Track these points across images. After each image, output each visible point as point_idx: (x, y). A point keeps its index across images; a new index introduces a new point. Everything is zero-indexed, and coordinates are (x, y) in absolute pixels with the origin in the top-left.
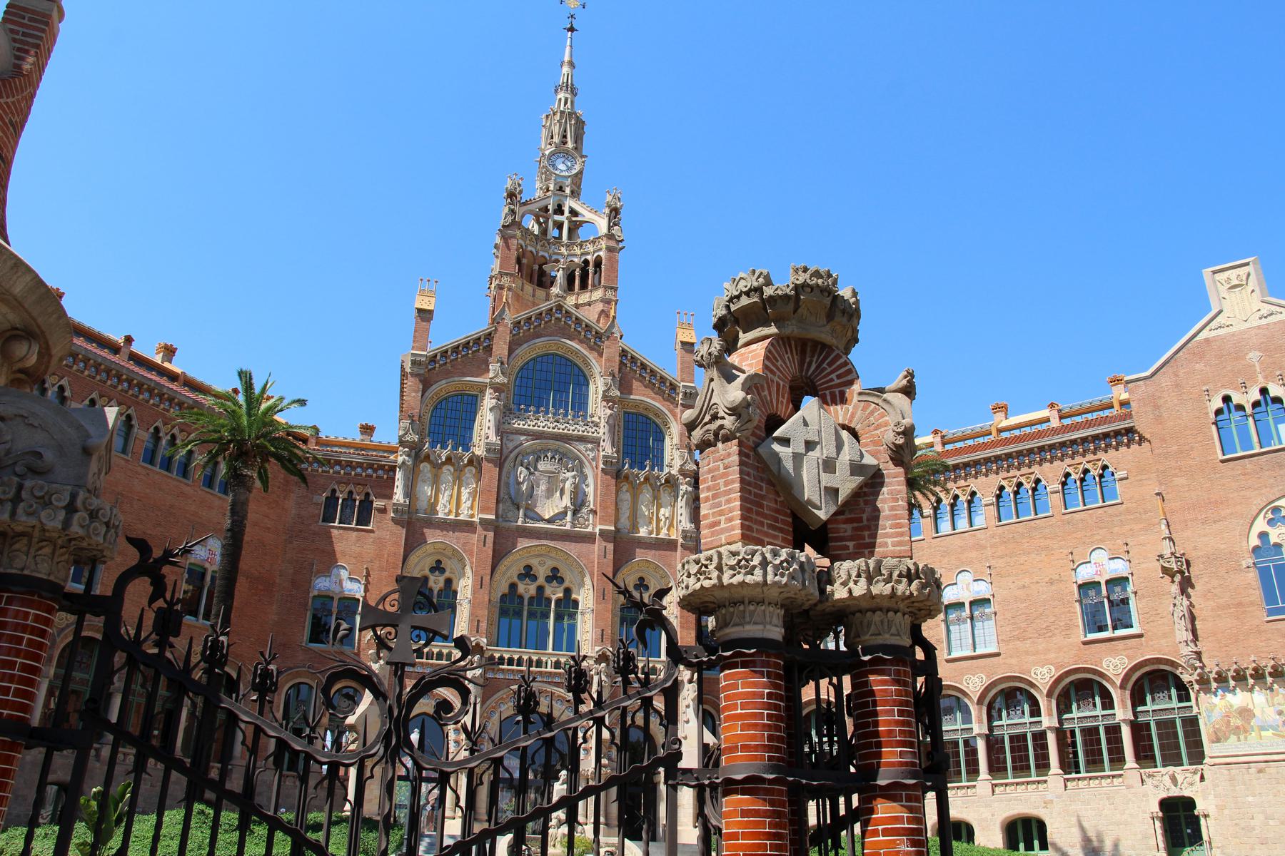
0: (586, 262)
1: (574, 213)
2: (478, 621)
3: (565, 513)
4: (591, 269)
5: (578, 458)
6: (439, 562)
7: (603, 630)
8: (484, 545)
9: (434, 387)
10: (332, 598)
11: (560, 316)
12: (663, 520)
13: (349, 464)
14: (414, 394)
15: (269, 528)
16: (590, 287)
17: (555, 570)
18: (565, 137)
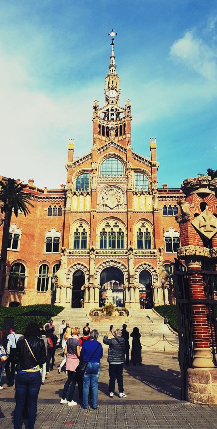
0: (121, 126)
1: (117, 110)
2: (93, 241)
3: (118, 206)
4: (123, 129)
5: (121, 189)
6: (81, 224)
7: (131, 241)
8: (93, 218)
9: (76, 172)
10: (52, 238)
11: (112, 145)
12: (149, 205)
13: (54, 198)
14: (70, 175)
15: (31, 220)
16: (123, 135)
17: (116, 223)
18: (112, 84)
